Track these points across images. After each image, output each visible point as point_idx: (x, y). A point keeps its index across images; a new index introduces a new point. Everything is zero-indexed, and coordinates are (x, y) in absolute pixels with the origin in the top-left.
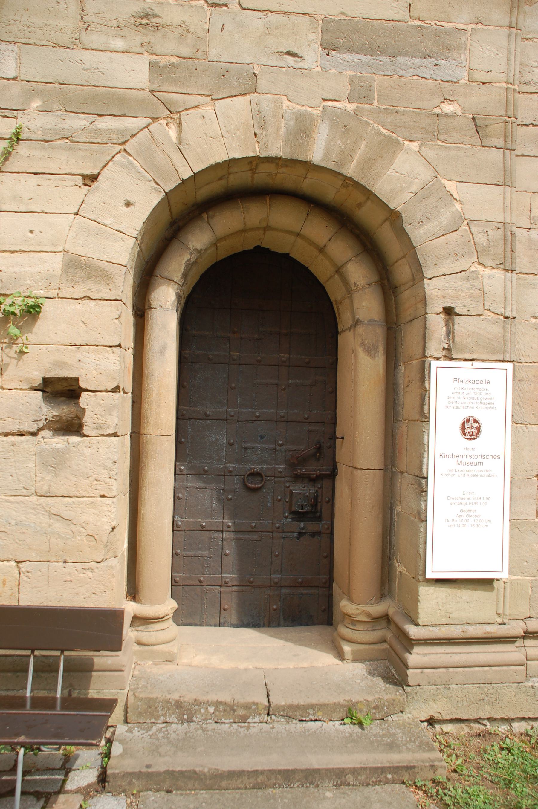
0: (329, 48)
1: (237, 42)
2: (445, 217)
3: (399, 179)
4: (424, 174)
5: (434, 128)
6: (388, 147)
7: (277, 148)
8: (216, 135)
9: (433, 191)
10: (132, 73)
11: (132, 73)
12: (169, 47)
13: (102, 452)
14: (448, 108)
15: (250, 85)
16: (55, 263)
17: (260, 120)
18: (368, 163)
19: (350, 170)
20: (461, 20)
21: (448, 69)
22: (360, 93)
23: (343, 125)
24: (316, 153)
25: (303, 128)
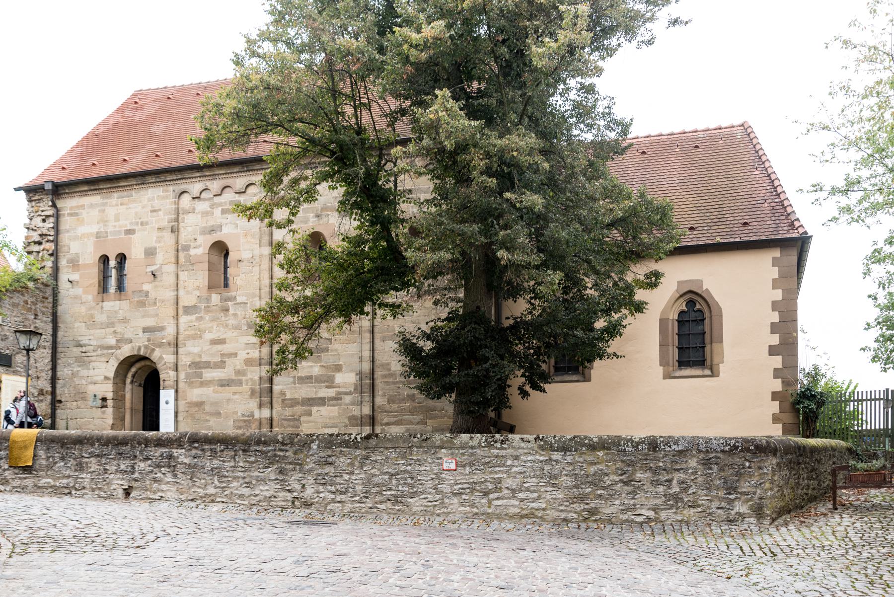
1: (128, 335)
5: (161, 345)
6: (153, 350)
8: (126, 351)
9: (161, 358)
11: (113, 342)
12: (119, 337)
15: (131, 341)
16: (102, 377)
20: (166, 324)
21: (165, 333)
22: (149, 340)
23: (146, 347)
25: (139, 348)
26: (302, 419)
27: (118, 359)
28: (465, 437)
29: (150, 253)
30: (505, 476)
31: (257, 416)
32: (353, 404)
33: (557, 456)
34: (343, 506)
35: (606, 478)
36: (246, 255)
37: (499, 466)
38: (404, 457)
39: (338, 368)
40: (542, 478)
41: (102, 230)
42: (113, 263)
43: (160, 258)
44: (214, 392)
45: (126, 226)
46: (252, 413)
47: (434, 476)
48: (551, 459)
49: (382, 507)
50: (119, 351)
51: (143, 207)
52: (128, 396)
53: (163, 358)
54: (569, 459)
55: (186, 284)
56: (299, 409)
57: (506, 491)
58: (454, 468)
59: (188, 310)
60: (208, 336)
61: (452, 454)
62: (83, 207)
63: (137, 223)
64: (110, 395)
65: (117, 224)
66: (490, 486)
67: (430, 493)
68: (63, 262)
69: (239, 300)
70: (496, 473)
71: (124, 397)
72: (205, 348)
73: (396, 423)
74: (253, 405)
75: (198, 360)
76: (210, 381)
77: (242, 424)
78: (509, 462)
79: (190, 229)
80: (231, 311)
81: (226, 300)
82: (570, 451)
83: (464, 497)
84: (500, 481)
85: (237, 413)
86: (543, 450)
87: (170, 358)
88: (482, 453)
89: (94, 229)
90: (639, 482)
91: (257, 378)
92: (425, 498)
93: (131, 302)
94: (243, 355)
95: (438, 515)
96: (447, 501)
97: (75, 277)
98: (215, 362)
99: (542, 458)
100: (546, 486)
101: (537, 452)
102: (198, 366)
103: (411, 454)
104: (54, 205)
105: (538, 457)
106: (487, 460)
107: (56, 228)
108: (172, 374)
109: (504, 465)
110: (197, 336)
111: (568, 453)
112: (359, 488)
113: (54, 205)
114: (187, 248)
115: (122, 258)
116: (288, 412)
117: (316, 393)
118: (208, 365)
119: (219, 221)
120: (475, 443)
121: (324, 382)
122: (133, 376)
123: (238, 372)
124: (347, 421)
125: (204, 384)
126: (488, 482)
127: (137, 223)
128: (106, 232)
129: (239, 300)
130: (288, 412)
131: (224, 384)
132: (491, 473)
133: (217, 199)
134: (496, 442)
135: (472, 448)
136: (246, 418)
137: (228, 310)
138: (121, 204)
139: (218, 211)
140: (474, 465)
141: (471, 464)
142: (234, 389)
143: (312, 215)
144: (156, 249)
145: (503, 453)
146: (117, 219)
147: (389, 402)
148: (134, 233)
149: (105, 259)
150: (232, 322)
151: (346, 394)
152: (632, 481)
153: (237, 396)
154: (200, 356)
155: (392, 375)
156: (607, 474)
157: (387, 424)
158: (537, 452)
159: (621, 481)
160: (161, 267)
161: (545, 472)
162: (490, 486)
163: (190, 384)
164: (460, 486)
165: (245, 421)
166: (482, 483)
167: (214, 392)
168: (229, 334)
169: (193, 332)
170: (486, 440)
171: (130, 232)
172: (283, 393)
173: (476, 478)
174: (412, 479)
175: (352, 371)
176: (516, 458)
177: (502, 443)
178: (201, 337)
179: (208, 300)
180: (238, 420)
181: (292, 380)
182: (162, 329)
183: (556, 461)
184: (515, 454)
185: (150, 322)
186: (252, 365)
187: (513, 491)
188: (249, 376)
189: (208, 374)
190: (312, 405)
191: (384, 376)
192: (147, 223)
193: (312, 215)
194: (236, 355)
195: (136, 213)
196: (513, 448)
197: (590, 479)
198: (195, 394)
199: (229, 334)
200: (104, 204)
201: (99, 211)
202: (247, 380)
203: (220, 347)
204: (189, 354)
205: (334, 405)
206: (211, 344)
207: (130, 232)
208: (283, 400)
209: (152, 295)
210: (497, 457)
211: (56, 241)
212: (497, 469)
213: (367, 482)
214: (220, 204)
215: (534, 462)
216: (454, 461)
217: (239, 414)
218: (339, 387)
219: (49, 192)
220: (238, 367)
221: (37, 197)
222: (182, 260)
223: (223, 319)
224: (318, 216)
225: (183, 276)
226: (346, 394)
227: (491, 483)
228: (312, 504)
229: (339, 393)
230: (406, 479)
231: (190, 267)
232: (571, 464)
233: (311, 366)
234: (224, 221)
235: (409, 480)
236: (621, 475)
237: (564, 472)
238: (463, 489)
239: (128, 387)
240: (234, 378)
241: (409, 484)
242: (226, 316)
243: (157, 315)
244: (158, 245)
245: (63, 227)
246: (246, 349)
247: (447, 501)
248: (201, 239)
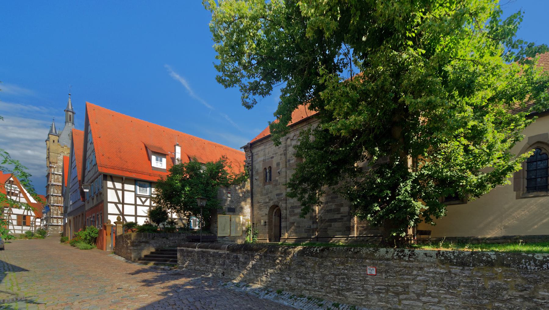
5: (281, 200)
10: (268, 200)
11: (268, 200)
13: (267, 226)
28: (383, 250)
29: (278, 164)
30: (412, 282)
33: (456, 270)
34: (310, 293)
35: (505, 292)
37: (407, 274)
38: (343, 264)
39: (342, 205)
40: (442, 287)
43: (281, 166)
47: (361, 278)
48: (450, 272)
49: (331, 295)
52: (274, 221)
53: (282, 205)
54: (467, 273)
57: (413, 295)
58: (375, 273)
61: (373, 263)
64: (267, 221)
66: (400, 289)
67: (359, 290)
68: (254, 173)
70: (405, 280)
71: (272, 221)
78: (415, 272)
82: (469, 266)
83: (381, 295)
84: (408, 286)
86: (443, 264)
87: (284, 205)
88: (395, 264)
90: (544, 299)
92: (356, 293)
95: (364, 306)
96: (370, 296)
97: (257, 177)
99: (442, 271)
100: (446, 294)
101: (438, 265)
103: (347, 263)
104: (251, 152)
105: (438, 270)
106: (398, 269)
107: (252, 160)
108: (285, 211)
109: (410, 274)
111: (466, 268)
112: (318, 282)
113: (251, 152)
114: (289, 161)
115: (270, 167)
120: (389, 256)
122: (275, 213)
125: (295, 215)
126: (399, 286)
127: (274, 154)
132: (401, 279)
134: (405, 256)
135: (388, 260)
140: (388, 272)
141: (386, 272)
145: (410, 264)
146: (268, 154)
149: (265, 169)
152: (534, 297)
156: (506, 289)
158: (438, 265)
159: (521, 296)
161: (445, 282)
162: (400, 289)
163: (291, 215)
164: (379, 287)
166: (394, 286)
170: (397, 254)
171: (272, 158)
173: (390, 282)
174: (348, 279)
176: (421, 269)
177: (409, 257)
182: (282, 194)
183: (455, 274)
184: (419, 266)
185: (278, 192)
187: (418, 295)
196: (418, 261)
197: (486, 292)
200: (265, 149)
204: (290, 203)
207: (272, 158)
209: (279, 181)
210: (405, 267)
211: (252, 165)
212: (406, 277)
213: (323, 277)
215: (435, 273)
216: (375, 269)
219: (250, 148)
222: (288, 166)
225: (288, 172)
227: (401, 287)
228: (294, 289)
230: (344, 278)
232: (468, 277)
235: (346, 280)
236: (522, 291)
237: (462, 284)
238: (380, 289)
239: (274, 217)
241: (346, 282)
245: (254, 159)
247: (370, 296)
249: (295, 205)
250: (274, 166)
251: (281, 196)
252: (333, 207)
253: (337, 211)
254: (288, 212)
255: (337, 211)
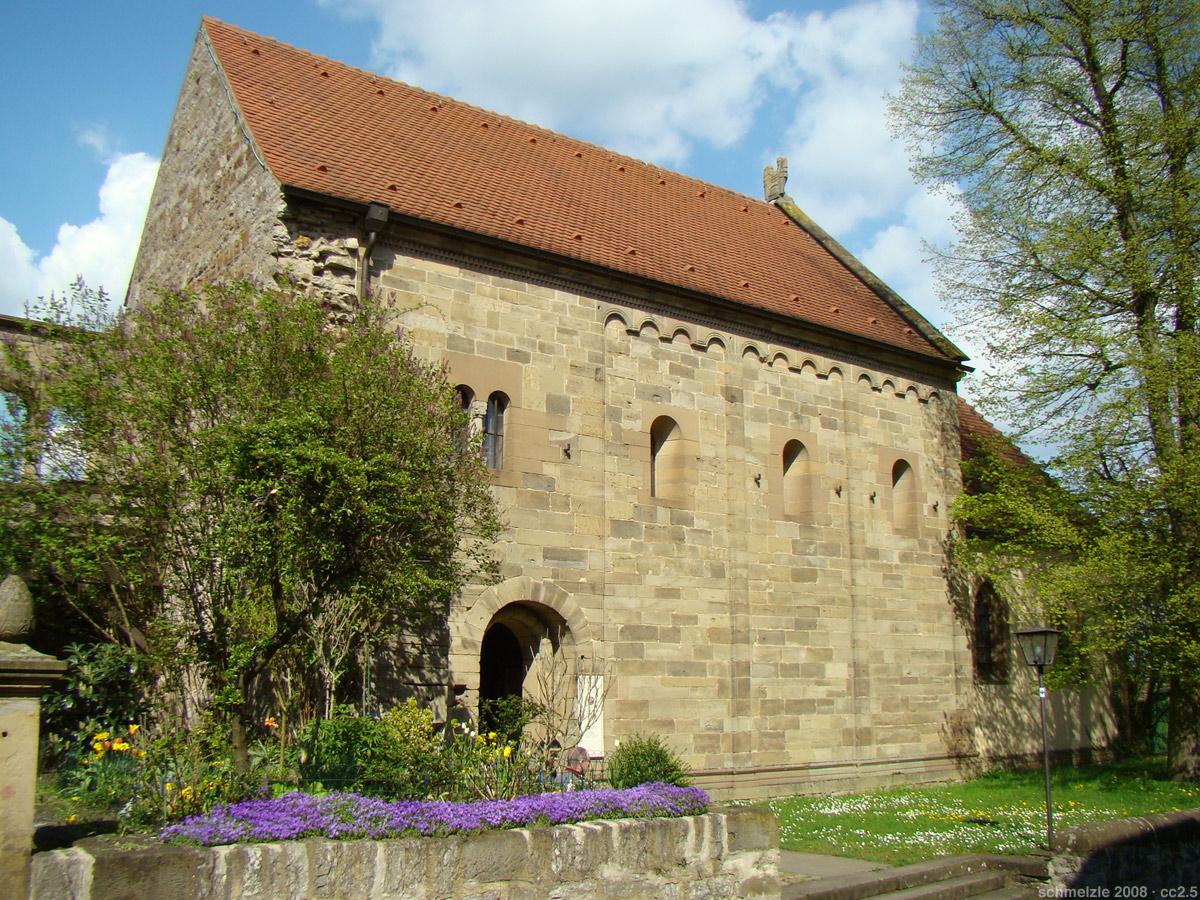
0: (545, 557)
2: (582, 621)
3: (567, 608)
4: (575, 605)
5: (577, 587)
6: (564, 596)
7: (529, 598)
9: (578, 612)
14: (583, 580)
17: (524, 586)
18: (558, 602)
19: (552, 605)
23: (550, 587)
24: (541, 600)
25: (537, 589)
26: (788, 733)
27: (491, 606)
29: (557, 406)
31: (728, 728)
32: (846, 711)
36: (707, 452)
39: (828, 655)
41: (461, 333)
42: (480, 405)
43: (576, 421)
44: (664, 682)
45: (511, 341)
46: (721, 723)
50: (495, 589)
51: (545, 317)
55: (616, 479)
56: (785, 717)
59: (621, 528)
60: (653, 581)
62: (420, 274)
63: (533, 344)
65: (492, 332)
69: (699, 524)
72: (649, 602)
73: (893, 740)
74: (721, 709)
75: (635, 622)
76: (656, 663)
77: (706, 743)
79: (621, 382)
80: (688, 543)
81: (679, 523)
85: (696, 723)
89: (443, 328)
91: (726, 663)
93: (520, 494)
94: (705, 621)
98: (663, 630)
102: (636, 633)
110: (635, 579)
115: (499, 400)
116: (769, 723)
117: (804, 690)
118: (651, 633)
119: (666, 382)
121: (811, 676)
123: (703, 652)
124: (840, 738)
125: (646, 668)
128: (471, 342)
129: (699, 524)
130: (769, 723)
131: (680, 669)
133: (663, 346)
136: (712, 733)
137: (682, 539)
138: (502, 298)
139: (664, 366)
142: (693, 679)
143: (790, 413)
144: (568, 403)
147: (883, 710)
148: (527, 361)
150: (688, 561)
151: (839, 695)
153: (698, 694)
154: (639, 615)
155: (884, 670)
157: (883, 741)
160: (576, 438)
165: (711, 737)
167: (664, 682)
168: (683, 582)
169: (627, 570)
172: (762, 692)
175: (843, 660)
178: (640, 581)
179: (652, 516)
180: (700, 737)
181: (773, 669)
182: (580, 556)
185: (559, 540)
186: (719, 640)
188: (716, 659)
189: (654, 651)
190: (799, 712)
191: (878, 671)
192: (551, 350)
193: (790, 413)
194: (694, 619)
195: (531, 325)
198: (633, 686)
199: (683, 582)
201: (457, 295)
202: (713, 666)
203: (670, 603)
204: (620, 609)
205: (826, 713)
206: (657, 596)
208: (764, 702)
209: (561, 487)
214: (668, 356)
217: (702, 725)
218: (828, 684)
220: (700, 642)
221: (312, 219)
223: (676, 554)
224: (797, 417)
226: (839, 695)
229: (831, 694)
231: (622, 451)
233: (797, 650)
234: (674, 385)
240: (693, 660)
242: (680, 549)
243: (571, 528)
244: (572, 396)
246: (710, 611)
248: (638, 406)
249: (646, 621)
250: (530, 395)
251: (572, 567)
252: (803, 657)
253: (815, 672)
254: (610, 651)
255: (815, 672)
